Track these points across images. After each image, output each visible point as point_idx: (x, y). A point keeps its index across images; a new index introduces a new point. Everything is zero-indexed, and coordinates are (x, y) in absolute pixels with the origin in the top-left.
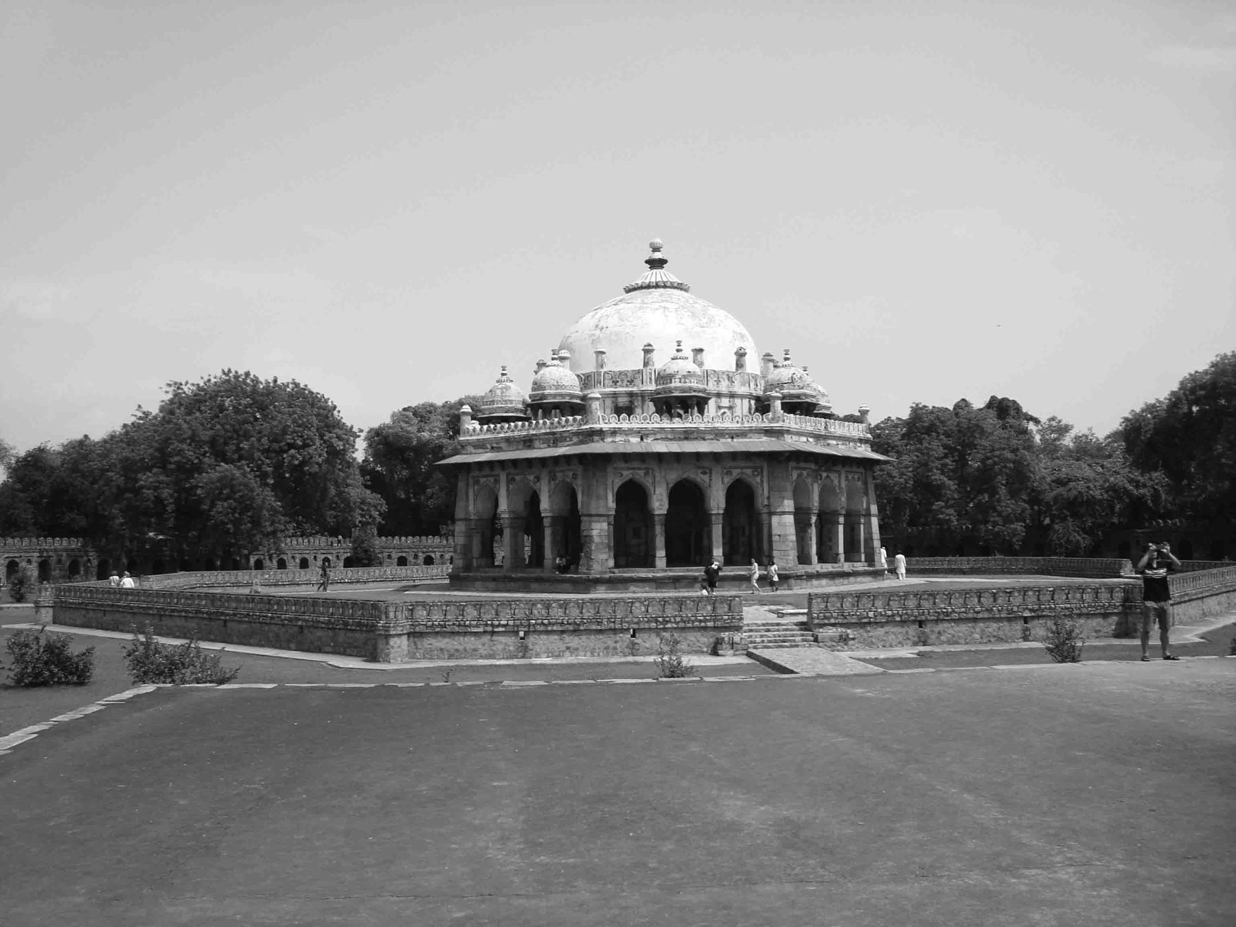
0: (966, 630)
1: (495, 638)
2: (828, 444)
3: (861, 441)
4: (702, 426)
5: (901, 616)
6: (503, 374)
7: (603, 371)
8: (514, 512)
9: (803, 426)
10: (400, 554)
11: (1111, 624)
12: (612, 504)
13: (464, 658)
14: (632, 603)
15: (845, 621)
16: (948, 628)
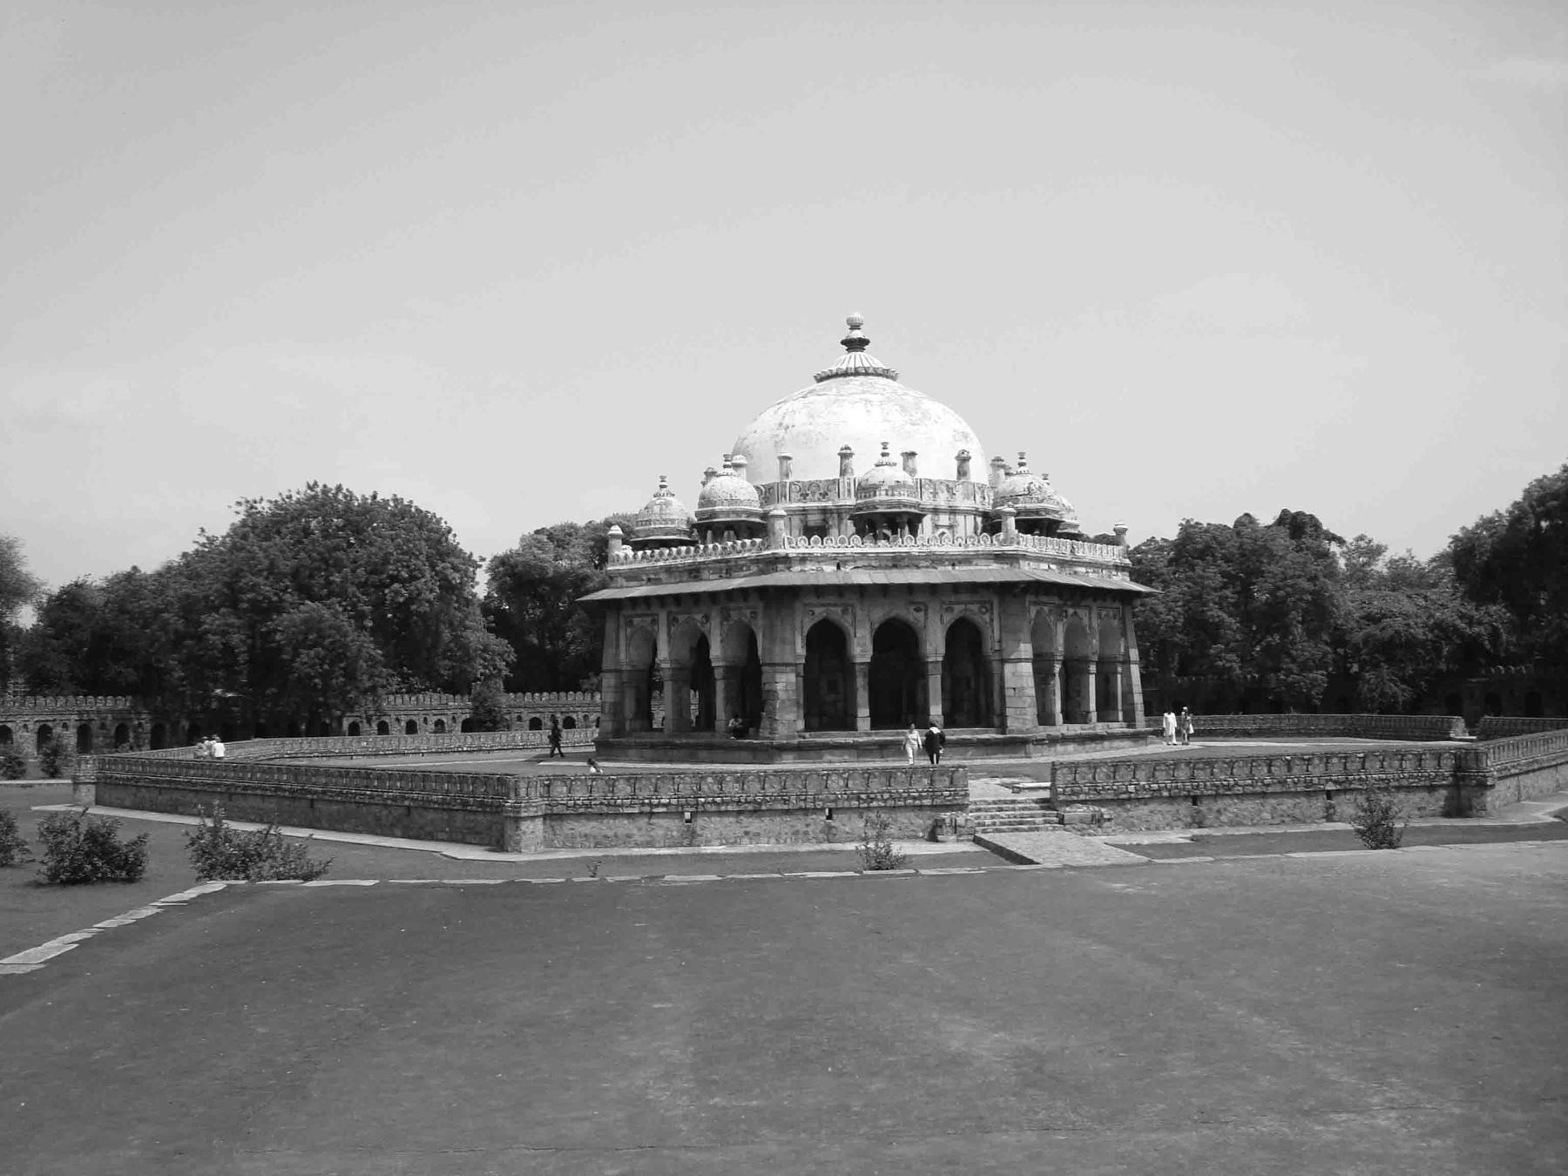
1: (653, 821)
2: (1075, 573)
3: (1117, 568)
4: (915, 550)
5: (1169, 790)
6: (662, 487)
7: (788, 481)
8: (677, 661)
10: (534, 715)
11: (1437, 801)
12: (801, 650)
13: (615, 846)
14: (828, 775)
15: (1098, 797)
16: (1230, 805)
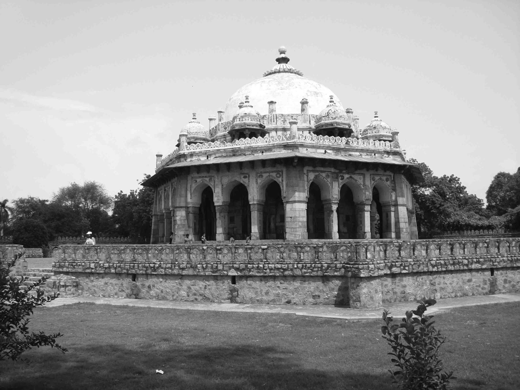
0: (174, 286)
2: (350, 155)
3: (388, 153)
4: (242, 147)
5: (115, 268)
7: (220, 123)
9: (321, 142)
11: (333, 289)
15: (74, 271)
